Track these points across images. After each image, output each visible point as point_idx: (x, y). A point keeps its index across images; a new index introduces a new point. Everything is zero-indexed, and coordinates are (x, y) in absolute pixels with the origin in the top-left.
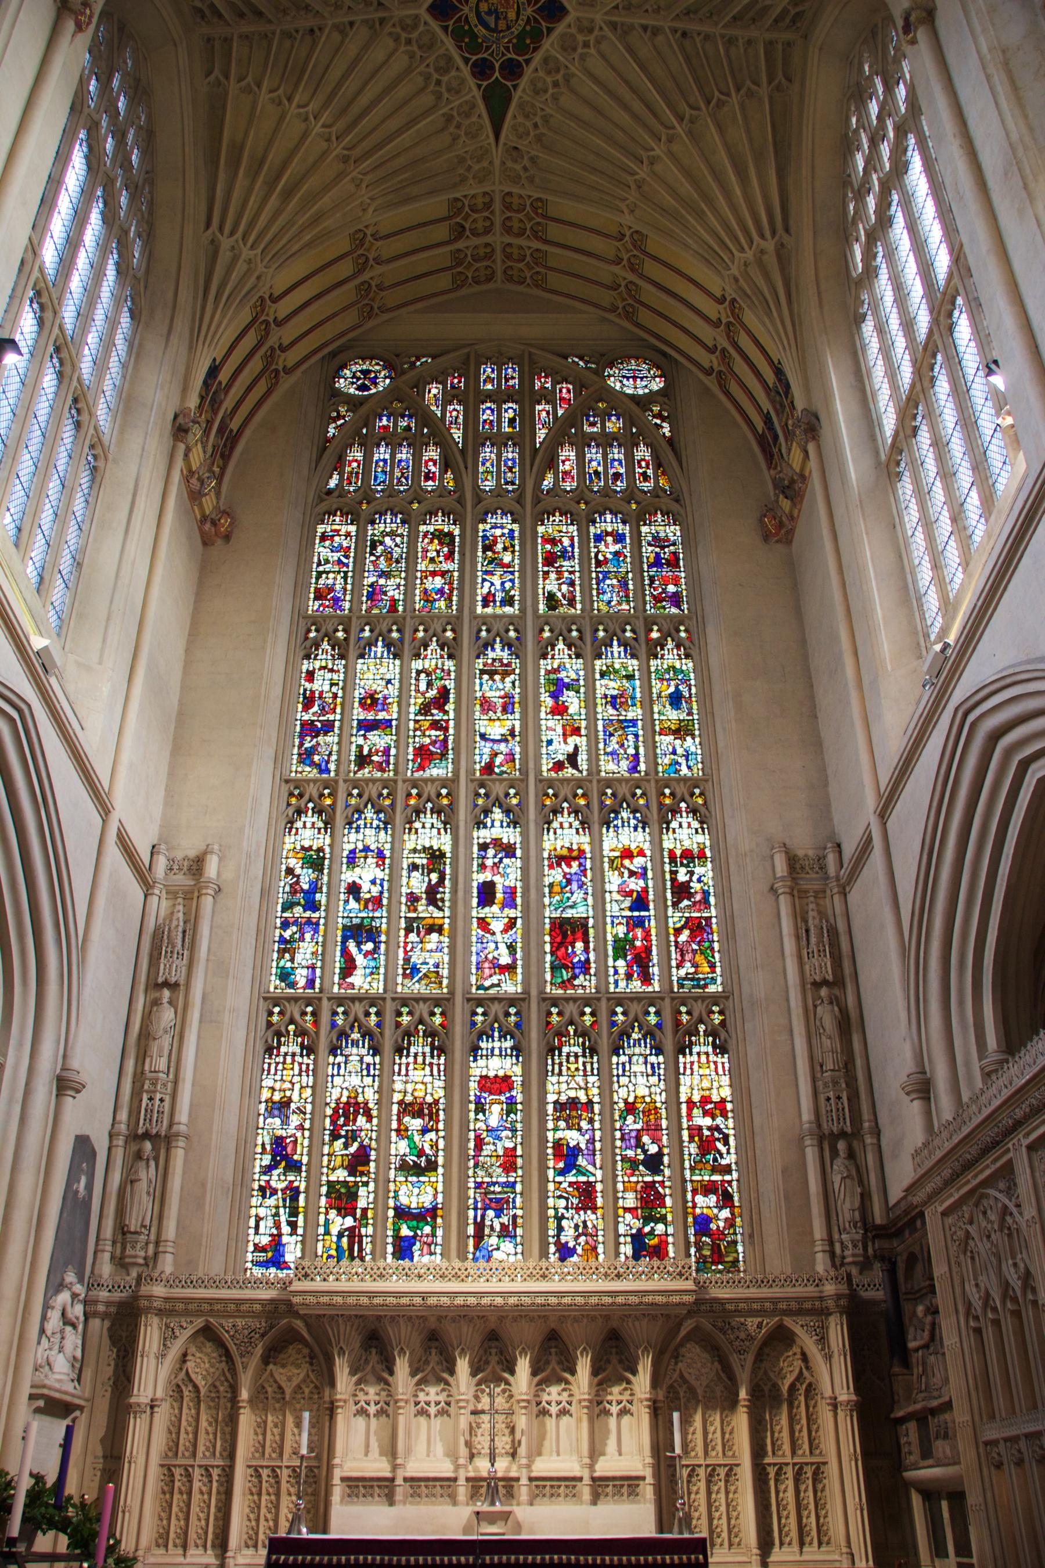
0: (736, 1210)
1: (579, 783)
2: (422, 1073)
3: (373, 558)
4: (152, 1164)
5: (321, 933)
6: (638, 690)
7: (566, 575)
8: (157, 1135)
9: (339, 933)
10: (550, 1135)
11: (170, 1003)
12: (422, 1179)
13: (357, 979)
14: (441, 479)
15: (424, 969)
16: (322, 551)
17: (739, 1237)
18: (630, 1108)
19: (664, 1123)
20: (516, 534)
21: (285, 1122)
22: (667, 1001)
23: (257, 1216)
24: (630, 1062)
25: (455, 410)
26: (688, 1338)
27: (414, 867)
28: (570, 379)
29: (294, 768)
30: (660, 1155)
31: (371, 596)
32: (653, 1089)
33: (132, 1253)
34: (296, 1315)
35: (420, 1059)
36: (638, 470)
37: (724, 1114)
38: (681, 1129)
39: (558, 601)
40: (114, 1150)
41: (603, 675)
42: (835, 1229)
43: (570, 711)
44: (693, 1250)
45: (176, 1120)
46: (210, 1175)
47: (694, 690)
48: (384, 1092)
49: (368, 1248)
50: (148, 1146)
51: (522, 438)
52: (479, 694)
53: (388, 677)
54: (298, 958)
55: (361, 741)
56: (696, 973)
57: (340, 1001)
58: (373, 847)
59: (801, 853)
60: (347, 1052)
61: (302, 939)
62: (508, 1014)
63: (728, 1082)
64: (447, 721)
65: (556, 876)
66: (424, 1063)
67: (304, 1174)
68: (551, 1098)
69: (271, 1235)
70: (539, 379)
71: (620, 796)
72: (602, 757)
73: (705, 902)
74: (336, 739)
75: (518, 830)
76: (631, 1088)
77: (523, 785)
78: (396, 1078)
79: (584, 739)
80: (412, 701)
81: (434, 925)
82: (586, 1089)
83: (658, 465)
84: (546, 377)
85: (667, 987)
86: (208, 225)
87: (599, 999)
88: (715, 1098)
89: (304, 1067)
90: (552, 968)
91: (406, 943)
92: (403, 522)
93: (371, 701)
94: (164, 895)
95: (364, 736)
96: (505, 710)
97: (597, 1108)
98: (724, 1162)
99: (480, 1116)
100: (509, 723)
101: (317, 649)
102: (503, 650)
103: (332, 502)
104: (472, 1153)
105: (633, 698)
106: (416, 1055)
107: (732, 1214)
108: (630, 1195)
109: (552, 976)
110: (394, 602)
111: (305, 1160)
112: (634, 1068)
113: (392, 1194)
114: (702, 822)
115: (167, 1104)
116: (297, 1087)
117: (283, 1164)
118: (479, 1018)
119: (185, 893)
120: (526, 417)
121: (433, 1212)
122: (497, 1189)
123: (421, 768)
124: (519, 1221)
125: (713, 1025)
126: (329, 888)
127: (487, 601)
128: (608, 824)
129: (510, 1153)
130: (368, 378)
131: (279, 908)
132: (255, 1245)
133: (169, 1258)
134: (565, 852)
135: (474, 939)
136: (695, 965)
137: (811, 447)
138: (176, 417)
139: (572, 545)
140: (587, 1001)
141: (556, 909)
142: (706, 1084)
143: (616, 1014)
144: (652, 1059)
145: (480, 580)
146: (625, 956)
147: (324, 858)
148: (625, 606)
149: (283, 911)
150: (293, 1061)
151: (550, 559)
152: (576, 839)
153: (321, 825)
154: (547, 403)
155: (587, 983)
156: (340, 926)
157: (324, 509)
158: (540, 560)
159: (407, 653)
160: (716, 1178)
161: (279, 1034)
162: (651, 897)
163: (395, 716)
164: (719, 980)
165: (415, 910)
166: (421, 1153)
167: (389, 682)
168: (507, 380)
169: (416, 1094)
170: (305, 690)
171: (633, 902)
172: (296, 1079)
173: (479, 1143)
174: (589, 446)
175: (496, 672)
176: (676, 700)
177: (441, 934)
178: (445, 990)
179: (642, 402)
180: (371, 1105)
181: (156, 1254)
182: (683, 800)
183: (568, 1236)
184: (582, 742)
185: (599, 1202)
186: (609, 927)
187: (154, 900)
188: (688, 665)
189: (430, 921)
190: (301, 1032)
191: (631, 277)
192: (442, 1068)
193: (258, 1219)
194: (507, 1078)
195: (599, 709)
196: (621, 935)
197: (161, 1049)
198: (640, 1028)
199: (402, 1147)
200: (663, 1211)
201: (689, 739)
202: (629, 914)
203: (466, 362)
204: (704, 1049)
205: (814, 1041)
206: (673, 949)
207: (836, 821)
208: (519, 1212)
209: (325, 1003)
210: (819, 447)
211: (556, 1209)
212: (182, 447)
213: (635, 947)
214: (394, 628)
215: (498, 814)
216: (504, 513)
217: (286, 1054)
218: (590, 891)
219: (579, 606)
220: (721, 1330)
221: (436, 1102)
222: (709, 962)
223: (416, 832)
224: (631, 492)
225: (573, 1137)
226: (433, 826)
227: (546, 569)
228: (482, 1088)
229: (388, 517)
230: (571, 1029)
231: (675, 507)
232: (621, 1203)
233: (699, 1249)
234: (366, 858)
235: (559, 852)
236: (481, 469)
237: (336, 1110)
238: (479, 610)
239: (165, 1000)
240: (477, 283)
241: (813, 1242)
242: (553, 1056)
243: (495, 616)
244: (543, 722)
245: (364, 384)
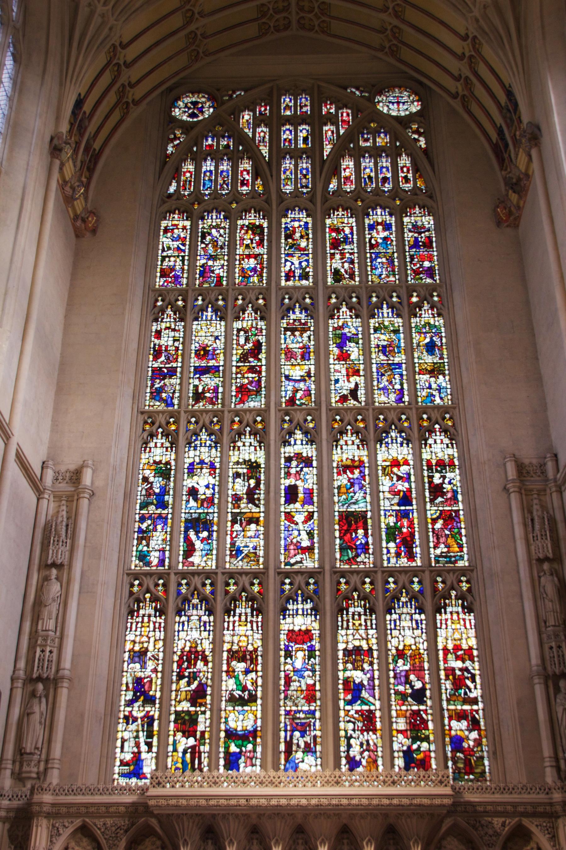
0: (482, 733)
1: (359, 411)
2: (245, 628)
3: (203, 246)
4: (44, 700)
5: (169, 525)
6: (402, 341)
7: (347, 255)
8: (48, 678)
9: (183, 525)
10: (341, 674)
11: (57, 579)
12: (246, 708)
13: (196, 559)
14: (253, 185)
15: (246, 550)
16: (165, 240)
17: (485, 754)
18: (400, 654)
19: (426, 665)
20: (310, 226)
21: (143, 666)
22: (427, 573)
23: (122, 738)
24: (400, 620)
25: (263, 131)
26: (448, 832)
28: (349, 105)
29: (147, 403)
30: (423, 689)
31: (202, 274)
32: (417, 639)
33: (28, 769)
34: (152, 815)
35: (243, 618)
36: (401, 175)
37: (472, 659)
38: (439, 670)
39: (342, 275)
40: (14, 690)
41: (376, 330)
42: (560, 749)
43: (352, 357)
44: (450, 764)
45: (62, 666)
46: (87, 707)
47: (444, 340)
48: (217, 643)
49: (205, 762)
50: (40, 686)
52: (283, 346)
53: (216, 334)
54: (152, 543)
55: (197, 382)
56: (448, 552)
57: (183, 575)
58: (207, 461)
59: (526, 461)
60: (189, 613)
61: (155, 530)
62: (308, 584)
63: (474, 634)
64: (260, 367)
65: (342, 480)
66: (246, 621)
67: (157, 706)
68: (341, 646)
69: (133, 753)
70: (326, 106)
71: (390, 421)
72: (376, 392)
73: (454, 499)
74: (178, 381)
75: (314, 446)
76: (401, 639)
77: (317, 413)
78: (225, 632)
79: (363, 378)
80: (234, 352)
81: (252, 518)
82: (367, 639)
84: (331, 104)
85: (427, 563)
87: (376, 572)
88: (465, 646)
89: (157, 625)
90: (341, 549)
91: (232, 532)
92: (225, 218)
94: (52, 499)
95: (199, 378)
96: (303, 358)
97: (375, 654)
98: (472, 695)
99: (289, 660)
100: (306, 367)
101: (163, 314)
102: (301, 313)
103: (172, 203)
104: (282, 688)
105: (399, 347)
106: (240, 615)
107: (480, 735)
108: (402, 720)
109: (341, 555)
110: (219, 278)
111: (158, 695)
112: (403, 624)
113: (223, 720)
114: (451, 439)
115: (55, 655)
116: (152, 640)
117: (142, 698)
118: (287, 587)
119: (68, 497)
121: (254, 733)
122: (302, 715)
123: (242, 401)
124: (319, 740)
125: (462, 591)
126: (174, 491)
127: (288, 276)
128: (381, 441)
129: (311, 688)
131: (138, 507)
132: (121, 761)
133: (56, 772)
134: (349, 463)
135: (282, 528)
136: (448, 546)
137: (534, 153)
138: (52, 139)
139: (352, 233)
140: (367, 573)
141: (343, 505)
142: (457, 636)
143: (389, 583)
144: (417, 617)
145: (283, 261)
146: (395, 540)
147: (170, 469)
148: (392, 278)
149: (141, 509)
150: (149, 621)
151: (335, 244)
152: (357, 453)
153: (168, 445)
154: (332, 124)
155: (367, 560)
156: (183, 519)
157: (166, 209)
158: (328, 245)
159: (230, 317)
160: (467, 707)
161: (138, 601)
162: (414, 495)
163: (222, 363)
164: (466, 557)
165: (239, 507)
166: (244, 689)
167: (217, 338)
168: (301, 107)
169: (241, 644)
170: (155, 345)
171: (400, 499)
172: (151, 634)
173: (288, 681)
174: (364, 157)
175: (296, 330)
177: (258, 525)
178: (261, 566)
180: (207, 653)
181: (46, 770)
182: (437, 423)
183: (355, 751)
184: (361, 380)
185: (378, 725)
186: (382, 518)
187: (44, 503)
188: (439, 322)
189: (250, 515)
190: (154, 599)
191: (395, 22)
192: (260, 624)
193: (123, 741)
194: (308, 631)
195: (374, 356)
196: (392, 524)
197: (50, 614)
198: (407, 593)
199: (229, 684)
200: (427, 733)
201: (441, 377)
202: (398, 508)
203: (270, 94)
204: (455, 609)
205: (539, 603)
206: (431, 534)
207: (553, 438)
208: (318, 733)
209: (173, 577)
211: (346, 731)
212: (57, 162)
213: (402, 533)
214: (220, 297)
215: (299, 435)
216: (301, 210)
217: (144, 615)
218: (368, 491)
219: (357, 279)
220: (474, 827)
221: (256, 650)
222: (458, 544)
223: (239, 450)
224: (396, 192)
225: (358, 676)
226: (251, 445)
227: (332, 251)
228: (290, 639)
229: (214, 214)
230: (355, 595)
231: (429, 202)
232: (394, 726)
233: (455, 763)
234: (201, 469)
235: (345, 462)
236: (283, 177)
237: (181, 657)
238: (283, 283)
239: (53, 577)
240: (278, 31)
241: (543, 759)
242: (342, 614)
243: (295, 288)
244: (332, 366)
245: (193, 113)
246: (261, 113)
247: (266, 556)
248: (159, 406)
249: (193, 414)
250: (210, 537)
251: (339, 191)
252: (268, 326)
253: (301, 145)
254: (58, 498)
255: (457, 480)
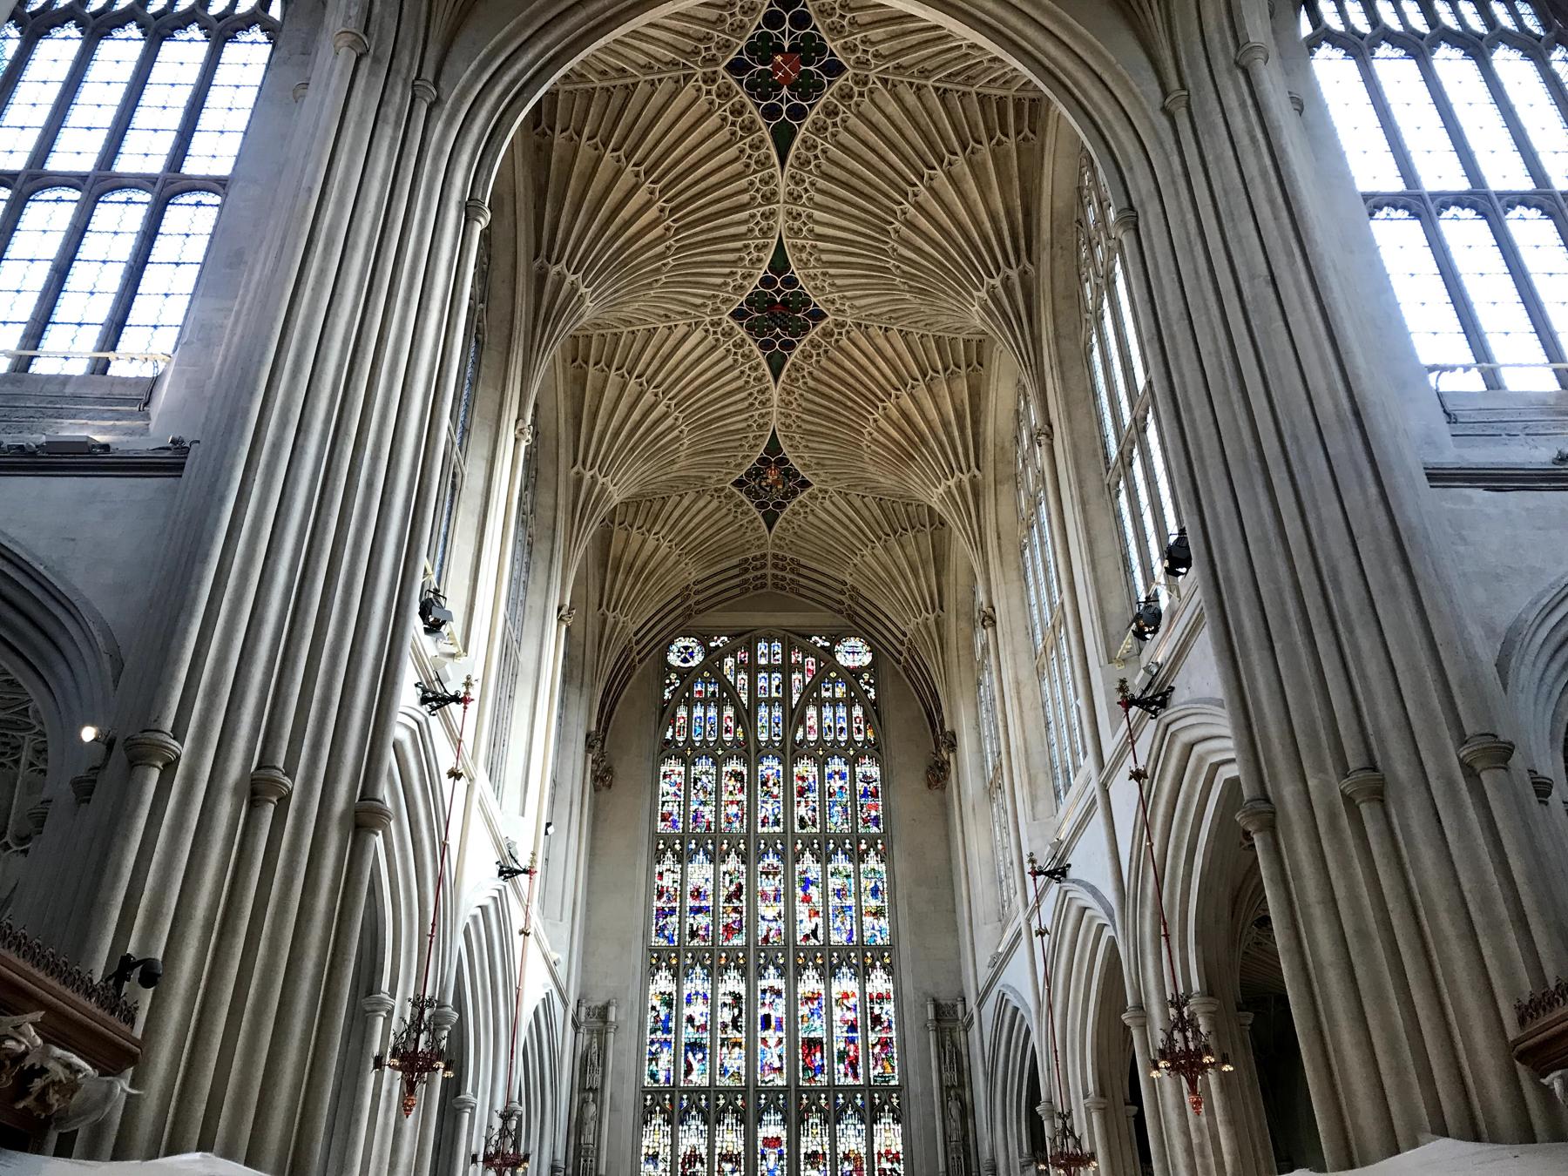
1: (815, 949)
13: (694, 1077)
16: (664, 786)
18: (846, 1157)
19: (865, 1166)
21: (656, 1167)
25: (743, 676)
27: (725, 1004)
31: (695, 819)
36: (855, 725)
41: (832, 875)
48: (711, 1147)
51: (785, 701)
55: (692, 921)
59: (943, 1002)
65: (804, 1010)
68: (803, 1151)
73: (890, 1027)
83: (866, 722)
86: (600, 606)
90: (804, 1070)
92: (713, 764)
93: (697, 894)
97: (828, 1157)
100: (777, 910)
110: (709, 823)
120: (786, 685)
123: (727, 939)
130: (687, 653)
136: (883, 1068)
142: (888, 1143)
144: (859, 1127)
161: (651, 1113)
176: (875, 892)
179: (856, 673)
184: (819, 921)
188: (882, 867)
190: (663, 1111)
210: (956, 757)
215: (772, 970)
221: (739, 1154)
228: (765, 1145)
236: (759, 724)
238: (760, 830)
246: (742, 662)
247: (747, 1075)
248: (663, 942)
249: (690, 950)
250: (704, 1058)
251: (804, 741)
252: (748, 869)
253: (774, 694)
254: (591, 1032)
255: (892, 1012)
